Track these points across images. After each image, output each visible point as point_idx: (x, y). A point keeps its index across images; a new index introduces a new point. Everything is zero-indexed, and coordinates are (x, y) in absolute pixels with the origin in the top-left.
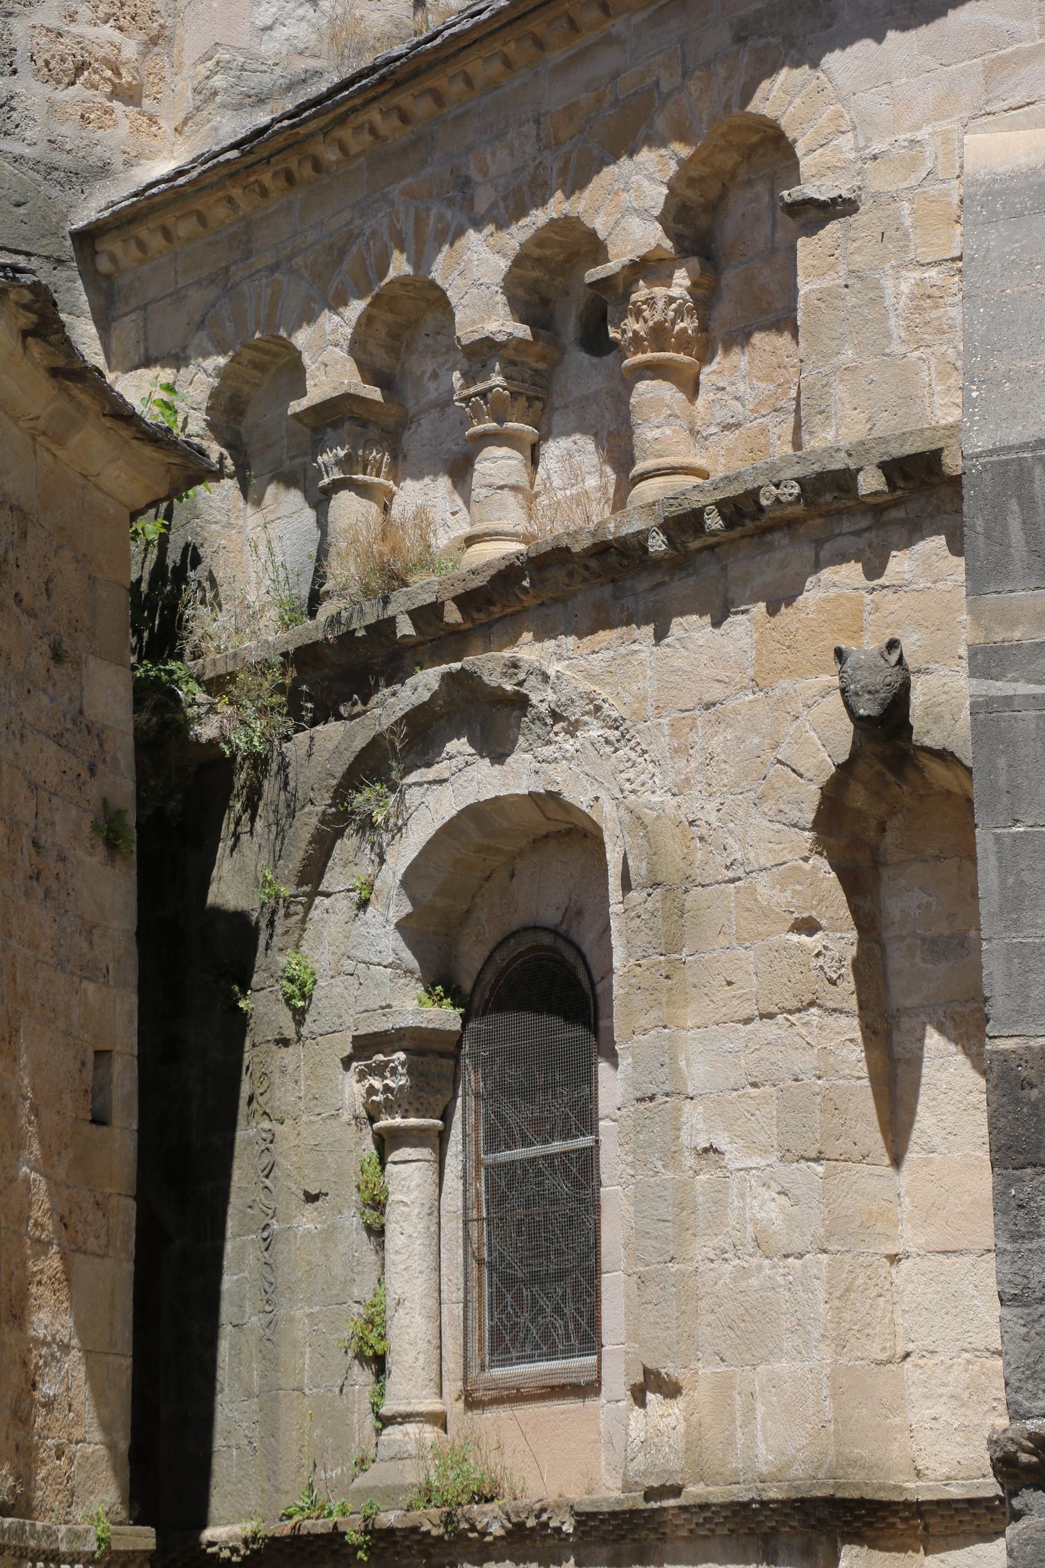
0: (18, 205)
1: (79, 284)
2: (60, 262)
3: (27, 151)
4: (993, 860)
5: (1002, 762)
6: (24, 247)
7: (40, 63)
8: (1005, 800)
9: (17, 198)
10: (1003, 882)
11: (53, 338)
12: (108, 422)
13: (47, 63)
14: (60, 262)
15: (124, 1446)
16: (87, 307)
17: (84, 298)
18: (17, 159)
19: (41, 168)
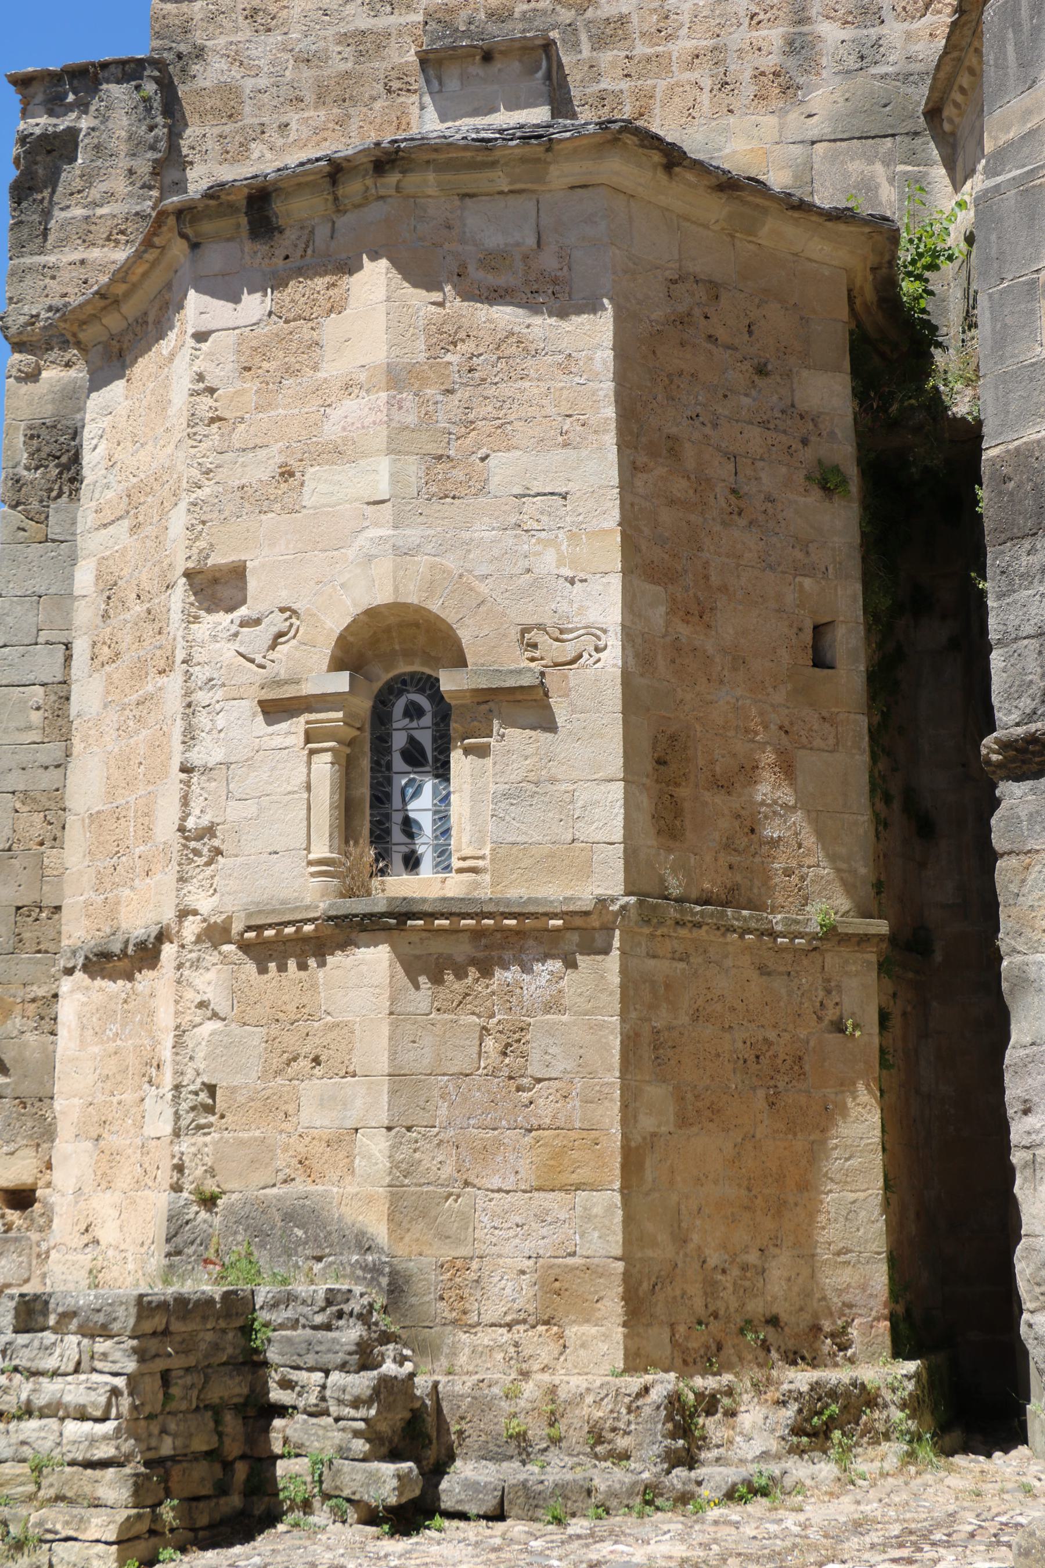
0: (885, 106)
1: (932, 145)
2: (916, 134)
3: (890, 69)
4: (987, 314)
5: (993, 237)
6: (890, 132)
7: (899, 9)
8: (995, 265)
9: (884, 101)
10: (993, 329)
11: (685, 163)
12: (790, 213)
13: (904, 8)
14: (916, 134)
15: (863, 870)
16: (938, 158)
17: (936, 152)
18: (883, 77)
19: (900, 77)
